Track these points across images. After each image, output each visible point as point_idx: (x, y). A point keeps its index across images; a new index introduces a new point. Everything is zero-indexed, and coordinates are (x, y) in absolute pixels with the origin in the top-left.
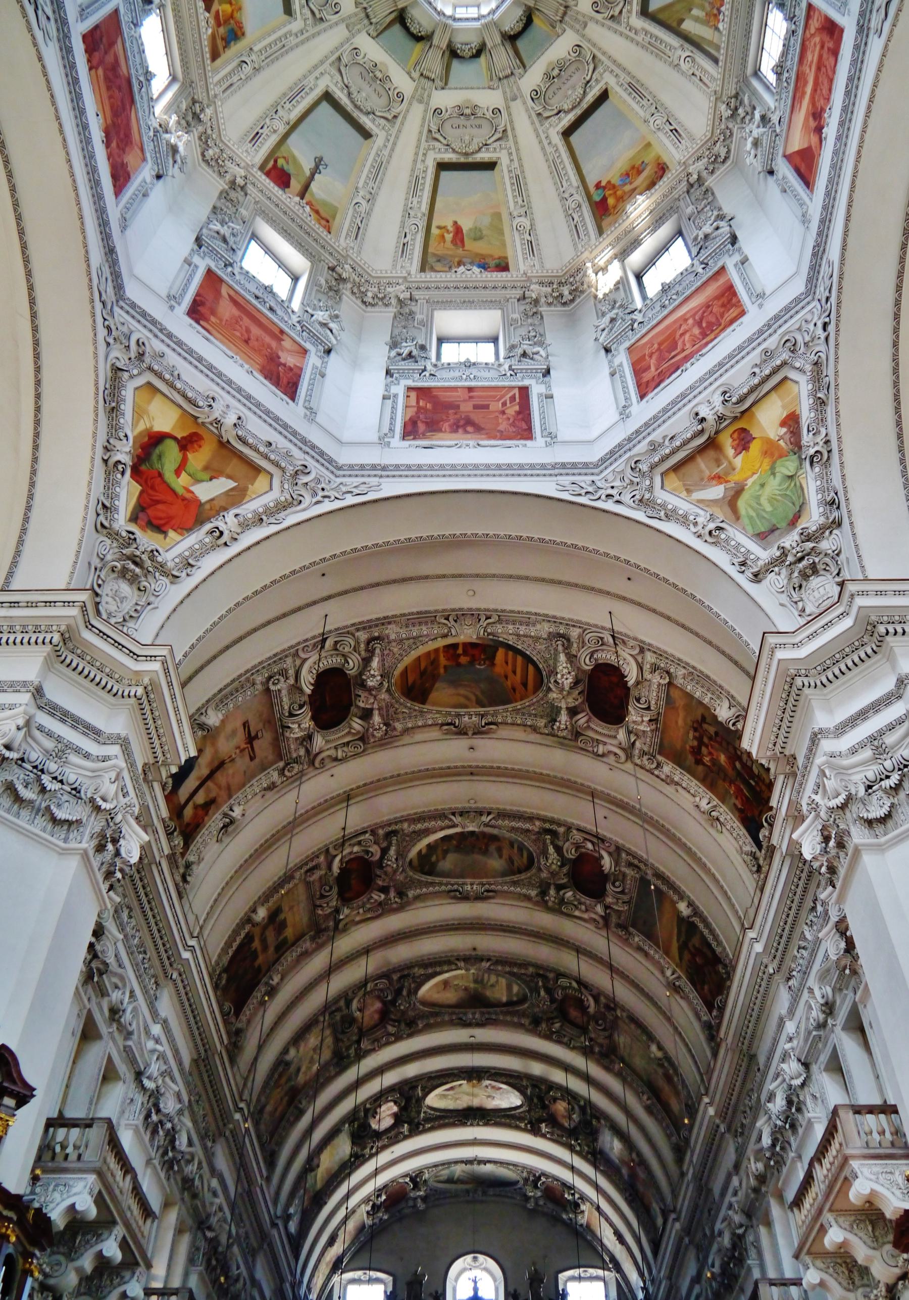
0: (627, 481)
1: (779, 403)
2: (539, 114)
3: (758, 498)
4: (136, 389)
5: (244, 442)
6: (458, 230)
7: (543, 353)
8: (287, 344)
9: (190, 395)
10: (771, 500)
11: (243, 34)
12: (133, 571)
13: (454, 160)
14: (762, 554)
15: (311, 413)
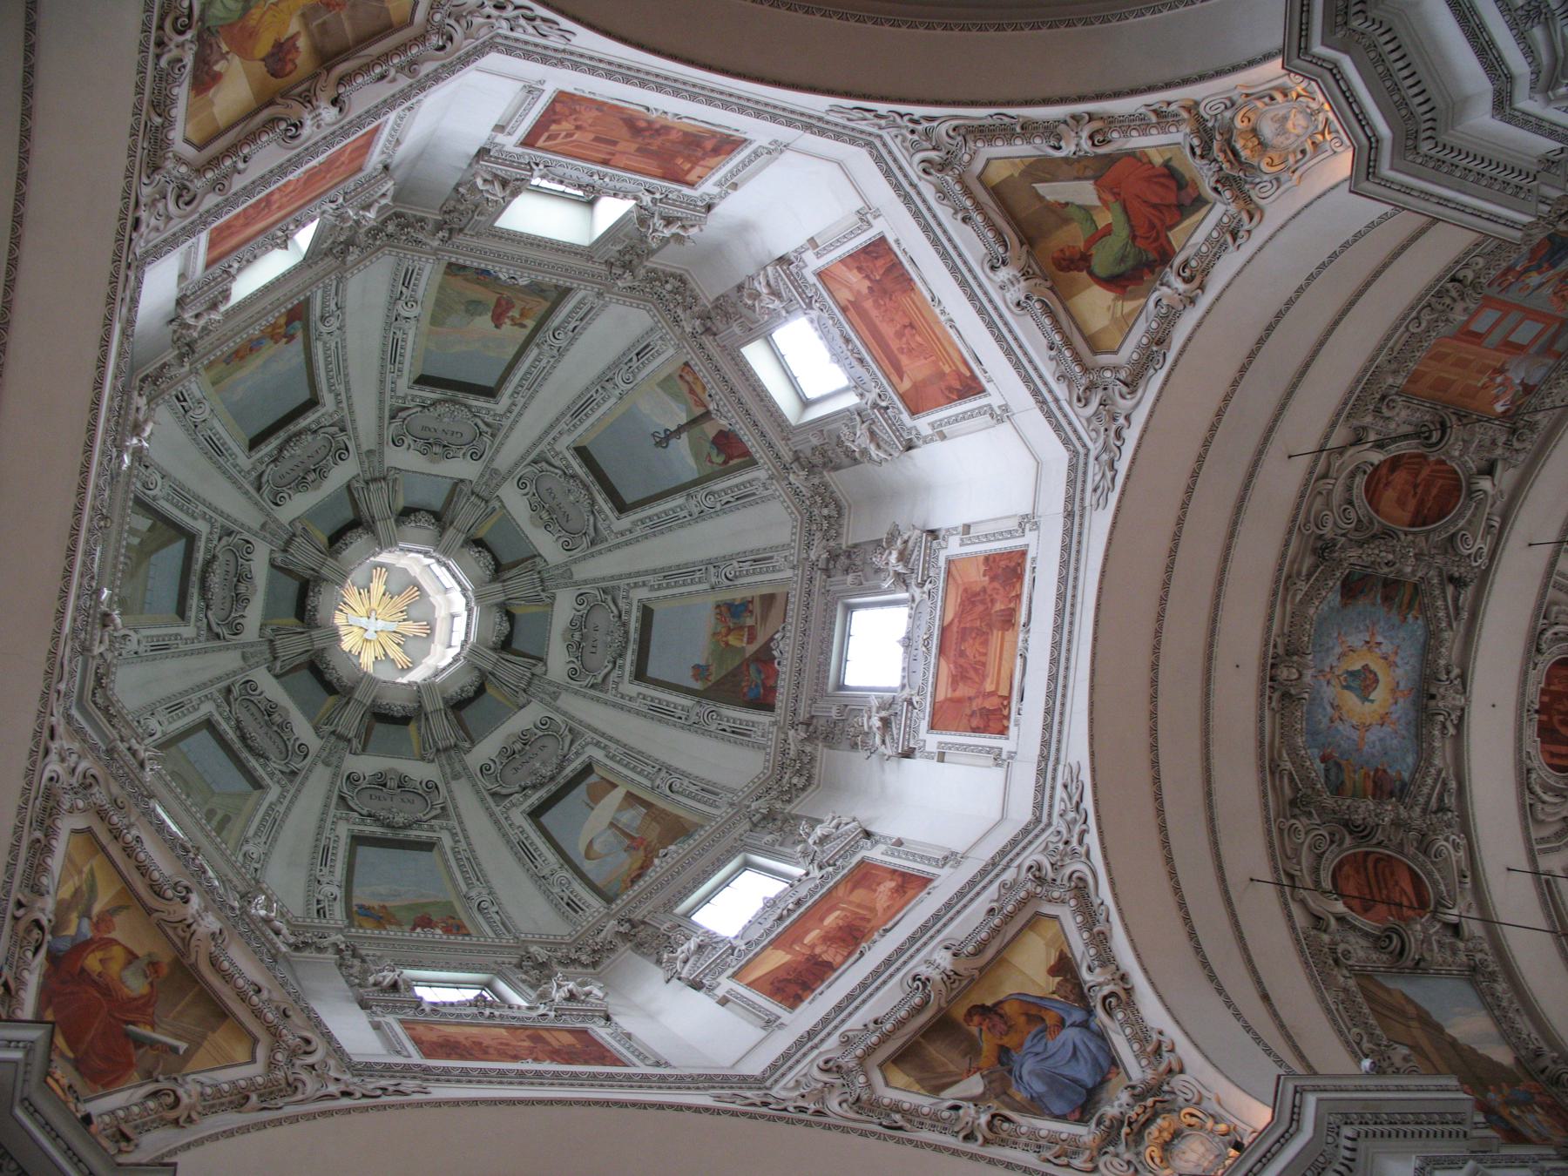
2: (343, 430)
5: (999, 235)
6: (498, 320)
9: (1047, 321)
11: (718, 606)
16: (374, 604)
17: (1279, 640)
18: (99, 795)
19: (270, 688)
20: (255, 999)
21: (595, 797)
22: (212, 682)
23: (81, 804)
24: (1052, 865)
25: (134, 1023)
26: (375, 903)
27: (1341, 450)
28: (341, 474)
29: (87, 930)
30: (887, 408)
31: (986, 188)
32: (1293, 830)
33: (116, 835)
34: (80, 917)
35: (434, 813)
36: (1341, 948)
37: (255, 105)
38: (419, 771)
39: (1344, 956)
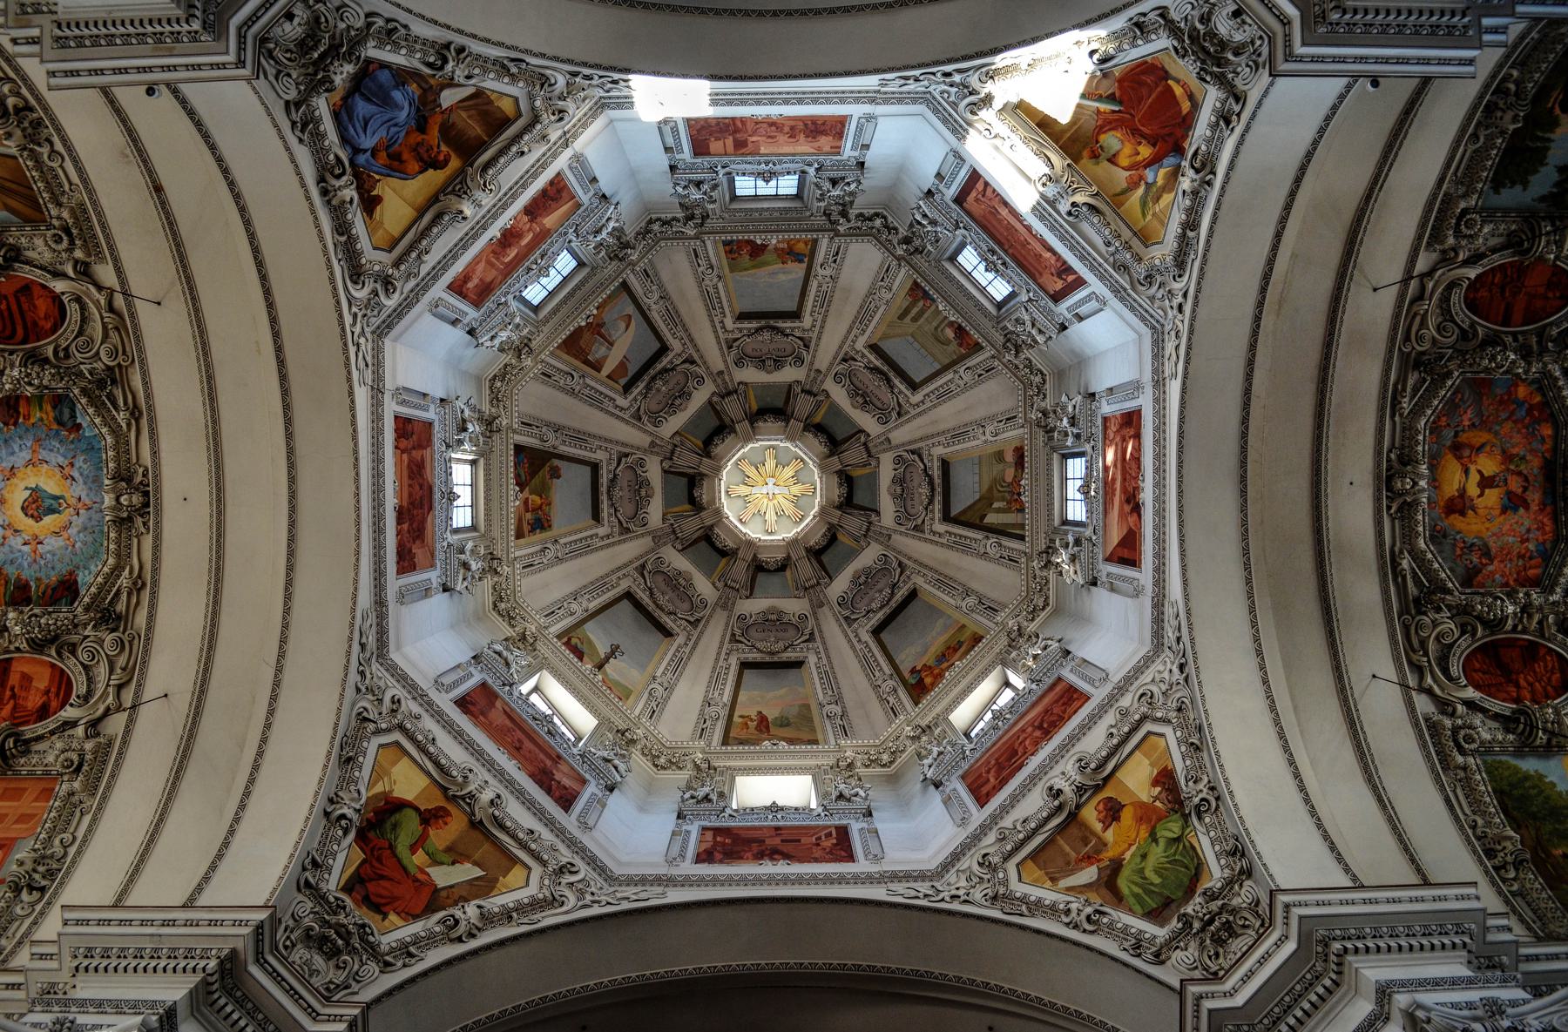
0: (975, 880)
1: (1147, 762)
2: (846, 618)
3: (1141, 871)
4: (381, 746)
5: (502, 827)
6: (762, 719)
7: (862, 793)
8: (563, 767)
9: (443, 761)
10: (1157, 872)
12: (334, 944)
13: (759, 660)
14: (1159, 932)
15: (586, 827)
16: (771, 504)
21: (622, 366)
24: (377, 295)
26: (791, 265)
29: (1149, 175)
30: (504, 685)
31: (522, 862)
34: (1155, 182)
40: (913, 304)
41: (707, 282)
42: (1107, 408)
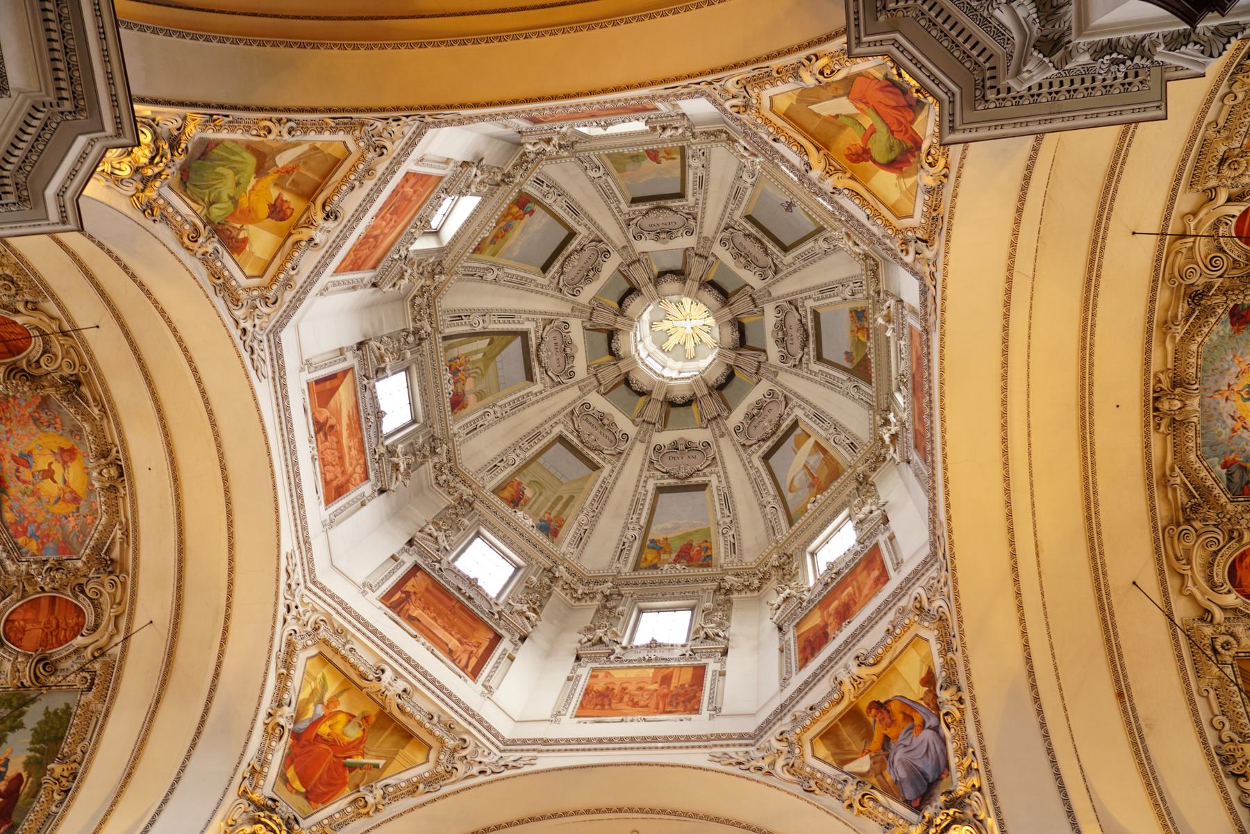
2: (600, 241)
4: (911, 217)
9: (857, 201)
16: (688, 310)
17: (1162, 377)
18: (323, 634)
19: (599, 403)
20: (428, 725)
21: (798, 445)
22: (559, 412)
23: (309, 643)
25: (350, 757)
27: (1195, 214)
28: (609, 267)
29: (320, 711)
32: (1183, 536)
33: (336, 651)
34: (315, 706)
35: (708, 462)
36: (1222, 639)
37: (282, 240)
38: (698, 435)
39: (1223, 647)
40: (560, 512)
41: (728, 520)
42: (367, 488)
